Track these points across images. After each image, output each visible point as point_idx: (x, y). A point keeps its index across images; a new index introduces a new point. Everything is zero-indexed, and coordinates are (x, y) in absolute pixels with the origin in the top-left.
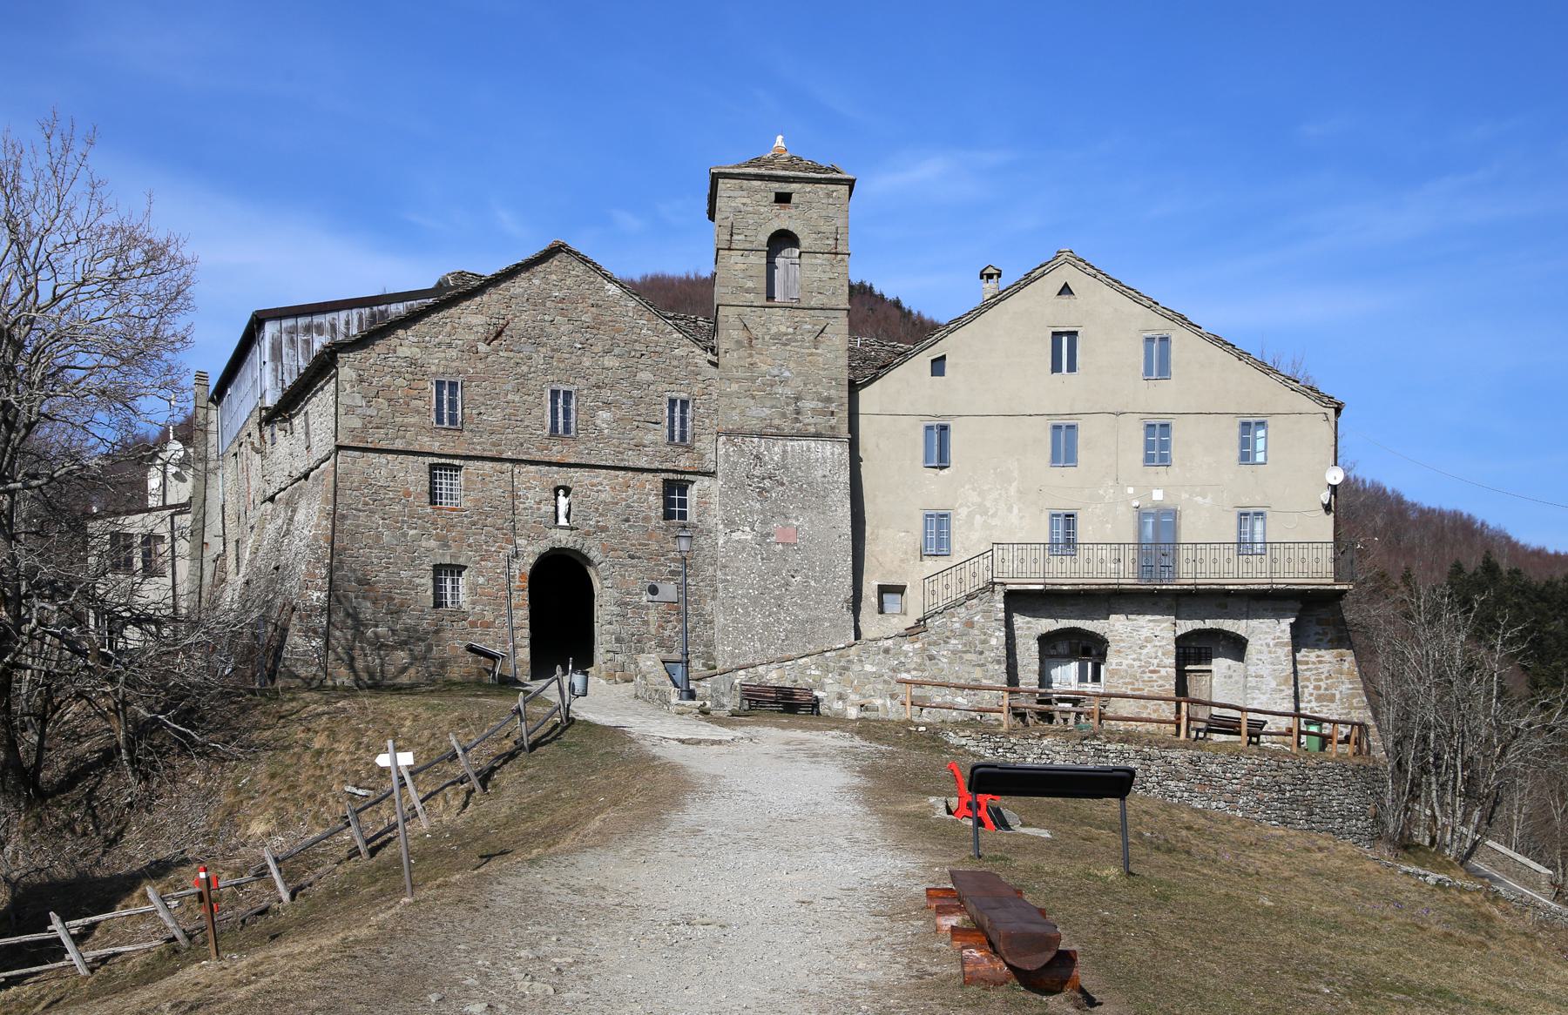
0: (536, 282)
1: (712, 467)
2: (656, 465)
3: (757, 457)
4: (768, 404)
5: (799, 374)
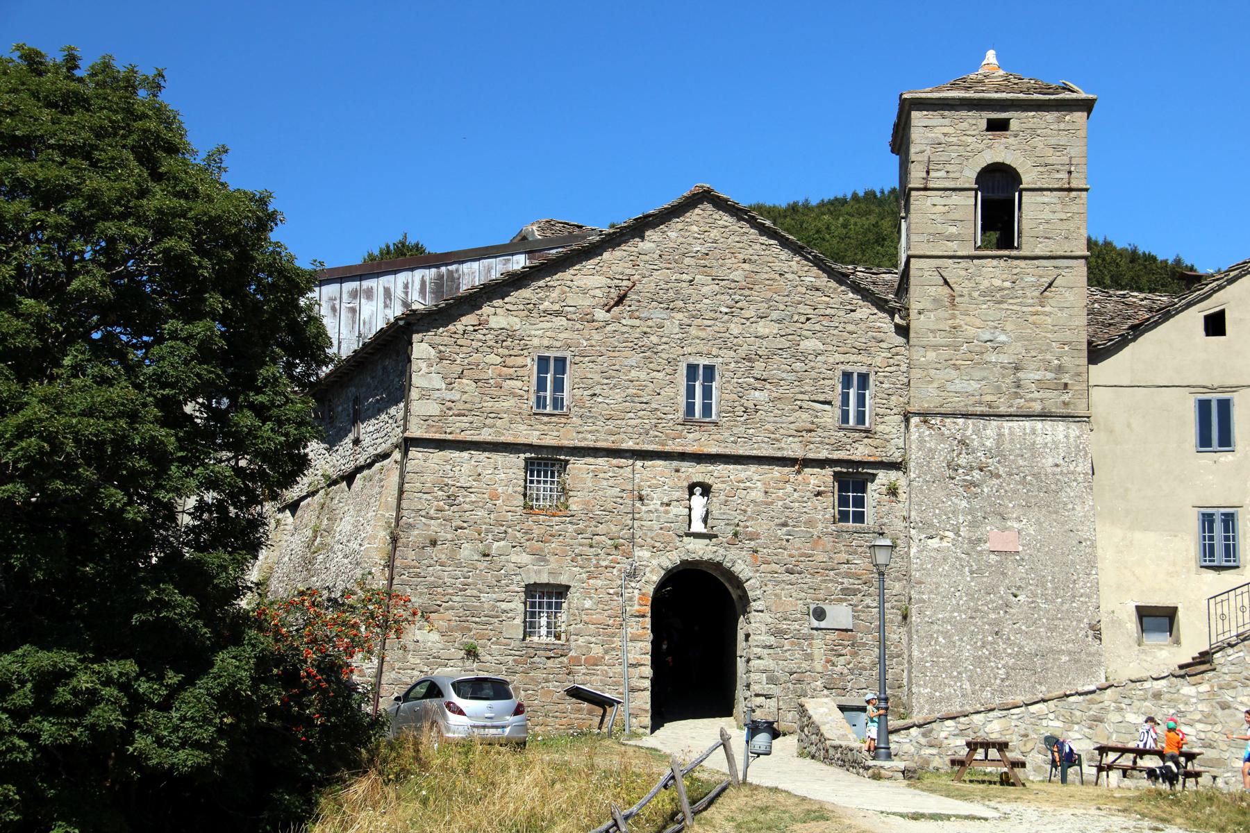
0: (673, 235)
1: (897, 457)
2: (823, 454)
3: (962, 442)
4: (977, 374)
5: (1018, 339)
